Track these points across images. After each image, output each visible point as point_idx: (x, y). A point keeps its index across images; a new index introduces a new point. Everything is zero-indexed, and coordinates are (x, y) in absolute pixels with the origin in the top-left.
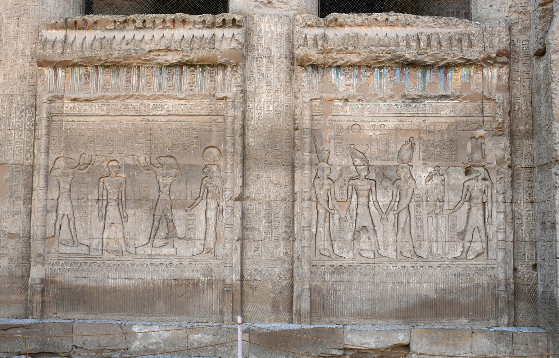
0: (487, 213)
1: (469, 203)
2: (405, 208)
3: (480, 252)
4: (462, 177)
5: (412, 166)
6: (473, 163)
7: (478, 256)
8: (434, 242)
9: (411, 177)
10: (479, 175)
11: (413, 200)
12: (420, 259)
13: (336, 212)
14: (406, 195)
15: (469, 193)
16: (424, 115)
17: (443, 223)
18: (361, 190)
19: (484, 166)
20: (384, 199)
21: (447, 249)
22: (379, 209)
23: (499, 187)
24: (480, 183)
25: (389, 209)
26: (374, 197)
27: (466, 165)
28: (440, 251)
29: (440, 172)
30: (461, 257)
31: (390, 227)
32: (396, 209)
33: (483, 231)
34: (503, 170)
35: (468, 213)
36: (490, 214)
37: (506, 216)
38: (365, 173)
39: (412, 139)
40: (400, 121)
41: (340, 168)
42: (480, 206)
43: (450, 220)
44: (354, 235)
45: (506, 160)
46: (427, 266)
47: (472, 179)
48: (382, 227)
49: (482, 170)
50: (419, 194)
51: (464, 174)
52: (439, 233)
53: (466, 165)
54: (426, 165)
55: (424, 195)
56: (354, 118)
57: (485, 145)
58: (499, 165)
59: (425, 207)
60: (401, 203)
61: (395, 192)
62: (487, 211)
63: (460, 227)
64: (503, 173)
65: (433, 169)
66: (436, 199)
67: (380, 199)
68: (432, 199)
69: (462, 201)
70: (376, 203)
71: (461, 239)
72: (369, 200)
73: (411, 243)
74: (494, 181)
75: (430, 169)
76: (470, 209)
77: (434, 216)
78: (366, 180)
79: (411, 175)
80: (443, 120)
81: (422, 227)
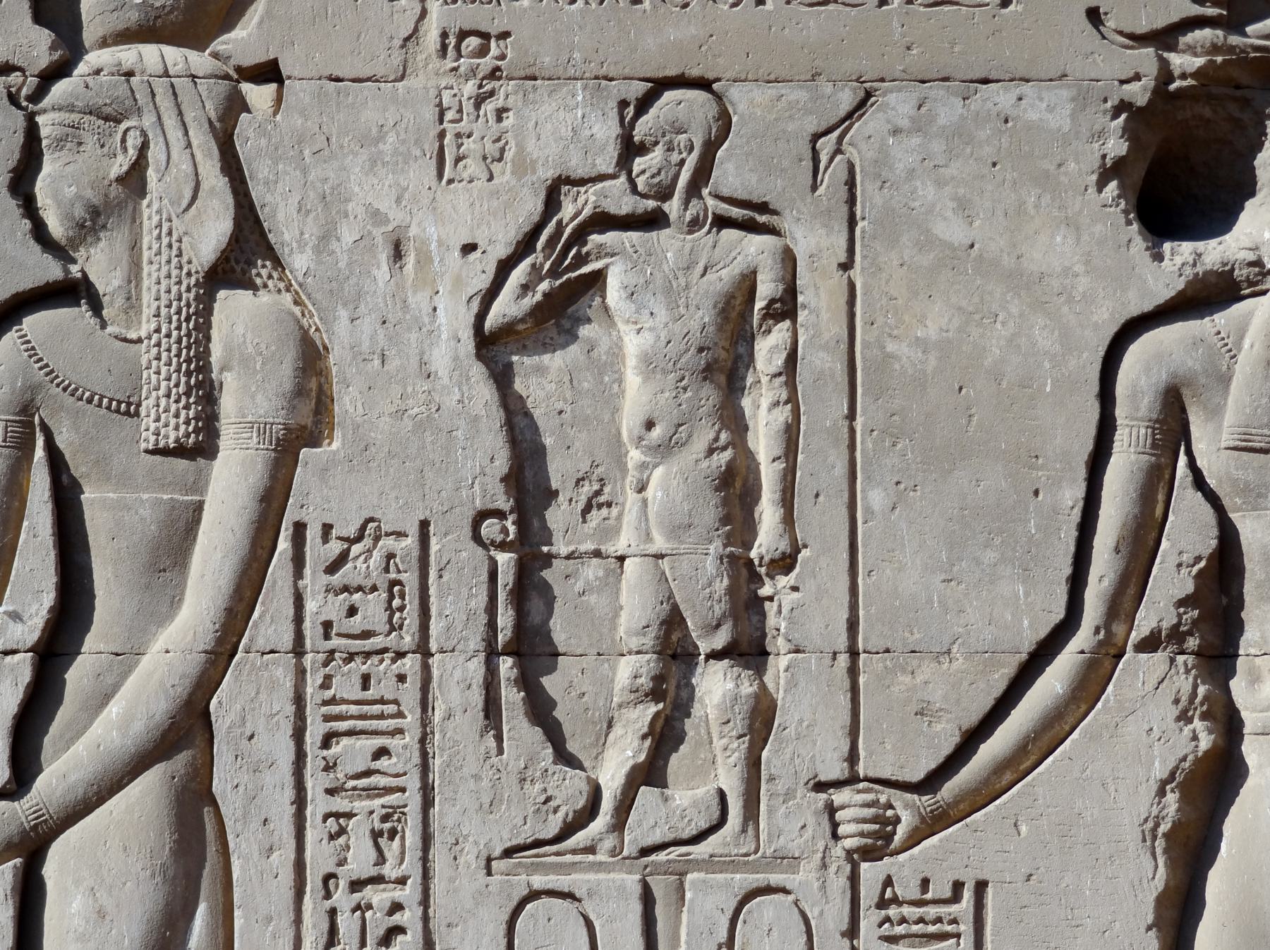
5: (269, 73)
29: (731, 174)
50: (368, 529)
65: (606, 130)
69: (1083, 639)
75: (566, 129)
77: (613, 894)
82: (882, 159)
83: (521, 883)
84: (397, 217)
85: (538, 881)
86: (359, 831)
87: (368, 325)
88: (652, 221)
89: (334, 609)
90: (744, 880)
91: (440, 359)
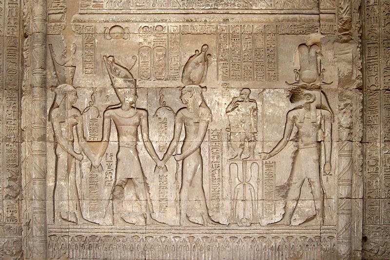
0: (323, 158)
1: (295, 143)
2: (193, 152)
3: (311, 214)
4: (284, 104)
6: (301, 83)
7: (307, 220)
8: (240, 202)
9: (203, 105)
10: (311, 100)
11: (206, 139)
12: (218, 227)
13: (85, 157)
14: (196, 132)
15: (295, 127)
16: (225, 11)
17: (254, 172)
18: (124, 125)
19: (319, 88)
20: (158, 138)
21: (259, 211)
22: (152, 153)
23: (344, 120)
24: (313, 113)
25: (169, 153)
26: (145, 135)
27: (291, 86)
28: (249, 214)
29: (251, 97)
30: (282, 222)
31: (170, 178)
32: (179, 152)
33: (317, 184)
34: (349, 93)
35: (294, 158)
36: (328, 159)
37: (352, 162)
38: (131, 100)
39: (205, 47)
40: (188, 21)
41: (91, 92)
42: (313, 149)
43: (265, 169)
44: (113, 191)
45: (354, 78)
46: (227, 237)
47: (300, 107)
48: (157, 180)
49: (317, 93)
50: (216, 130)
51: (288, 99)
52: (248, 187)
53: (291, 86)
54: (227, 87)
55: (224, 131)
56: (114, 17)
57: (322, 55)
58: (343, 87)
59: (225, 148)
60: (187, 143)
61: (177, 127)
62: (323, 153)
63: (281, 178)
64: (350, 98)
65: (238, 93)
66: (243, 137)
67: (155, 138)
68: (237, 138)
70: (148, 144)
71: (283, 196)
72: (137, 140)
73: (202, 203)
74: (336, 110)
75: (235, 93)
76: (297, 152)
77: (240, 163)
78: (132, 110)
79: (204, 101)
80: (255, 18)
81: (221, 180)
82: (266, 96)
83: (231, 162)
84: (218, 101)
85: (233, 162)
86: (215, 158)
87: (215, 111)
88: (243, 101)
89: (212, 137)
90: (252, 162)
91: (223, 114)
